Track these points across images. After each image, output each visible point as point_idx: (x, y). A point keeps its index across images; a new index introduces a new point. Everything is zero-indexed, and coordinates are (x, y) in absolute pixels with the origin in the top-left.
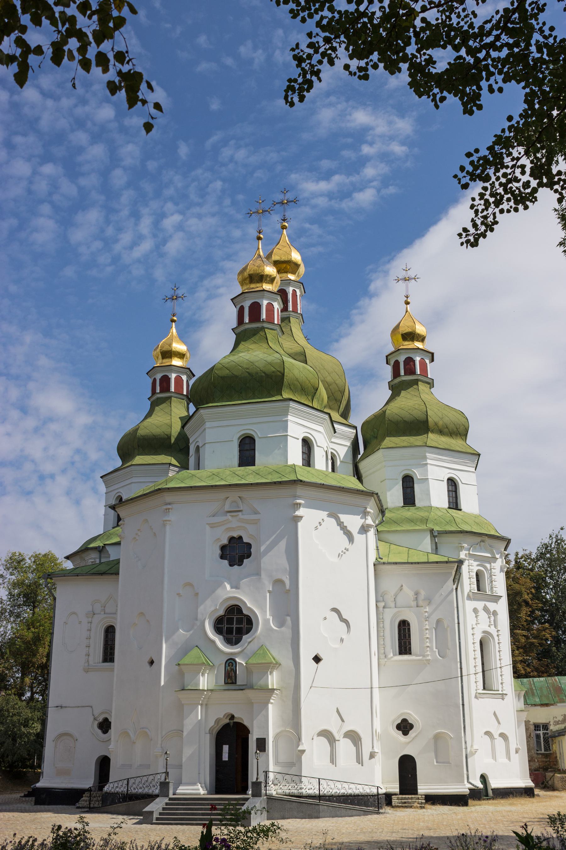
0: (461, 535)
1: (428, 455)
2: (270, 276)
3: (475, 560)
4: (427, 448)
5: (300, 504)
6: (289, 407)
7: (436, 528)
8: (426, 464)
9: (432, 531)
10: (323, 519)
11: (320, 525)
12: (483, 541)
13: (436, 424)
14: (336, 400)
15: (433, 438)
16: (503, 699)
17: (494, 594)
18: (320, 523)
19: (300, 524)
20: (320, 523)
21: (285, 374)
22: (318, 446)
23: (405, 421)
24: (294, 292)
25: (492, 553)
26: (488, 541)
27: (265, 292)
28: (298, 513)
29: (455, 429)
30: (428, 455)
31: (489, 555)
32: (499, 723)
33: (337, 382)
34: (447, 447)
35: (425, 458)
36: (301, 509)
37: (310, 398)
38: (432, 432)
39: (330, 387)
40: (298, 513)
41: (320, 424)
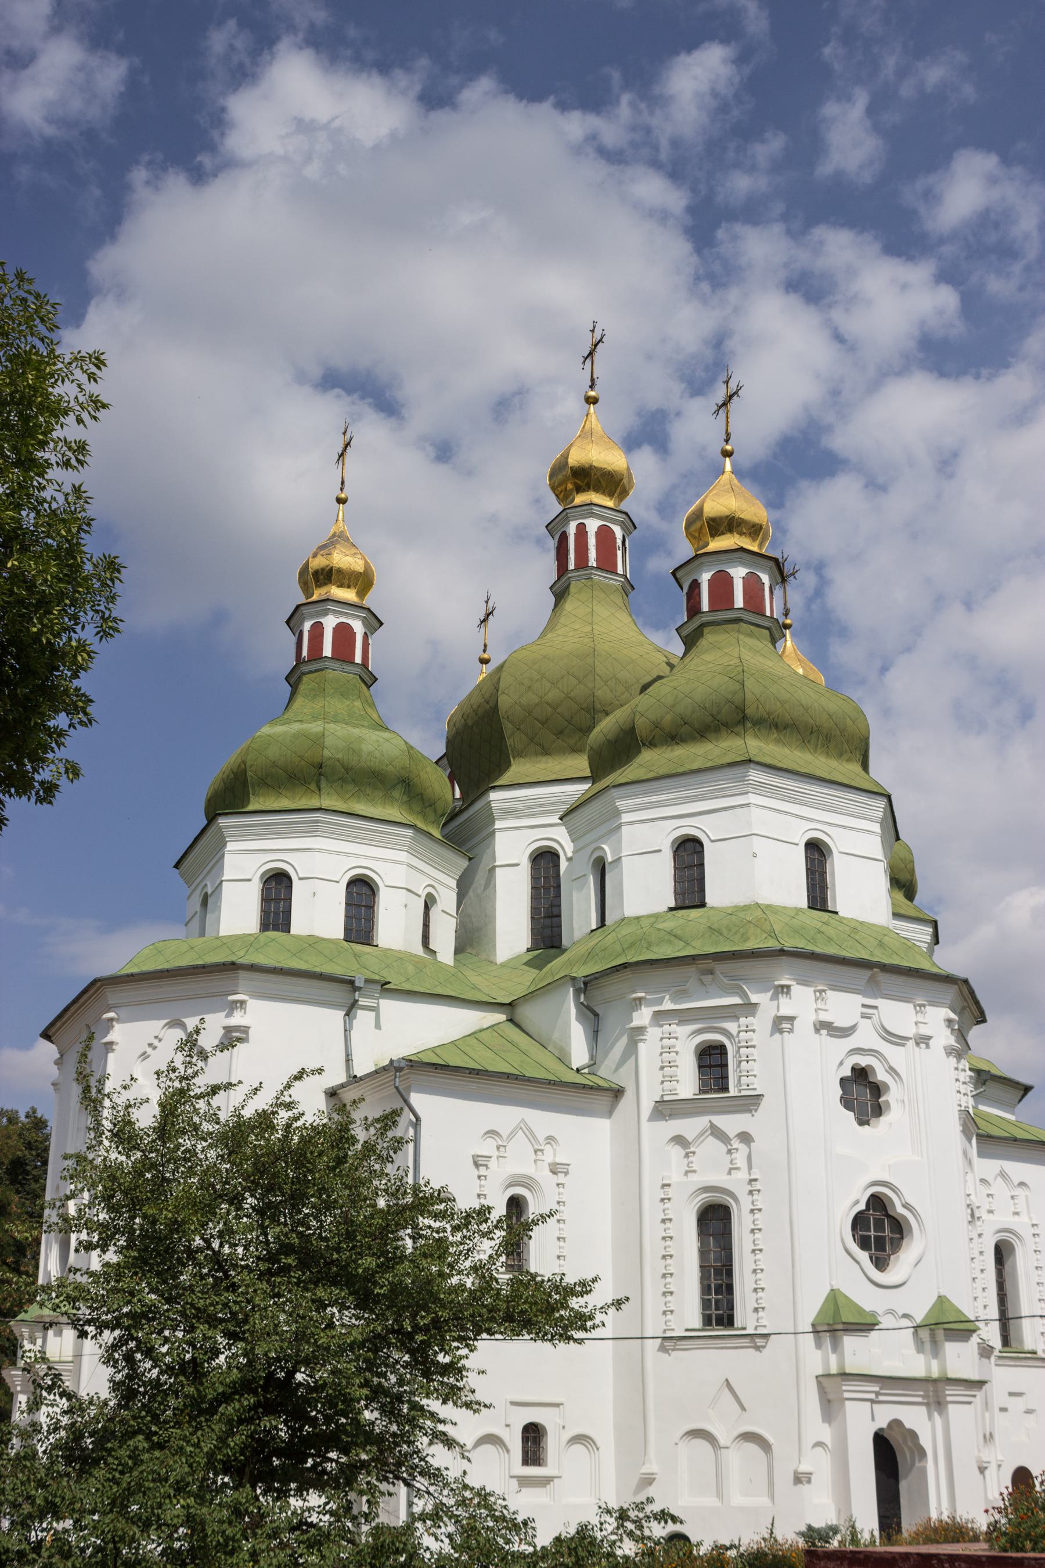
0: (627, 974)
1: (620, 804)
2: (323, 569)
3: (681, 1022)
4: (613, 790)
5: (112, 1020)
6: (220, 828)
7: (581, 972)
8: (619, 826)
9: (574, 979)
10: (156, 1037)
11: (155, 1048)
12: (711, 972)
13: (656, 725)
14: (581, 730)
15: (649, 760)
16: (758, 1348)
17: (743, 1093)
18: (150, 1045)
19: (111, 1056)
20: (150, 1045)
21: (248, 764)
22: (300, 879)
23: (608, 741)
24: (582, 529)
25: (744, 995)
26: (720, 968)
27: (302, 608)
28: (108, 1039)
29: (710, 718)
30: (620, 804)
31: (736, 1000)
32: (743, 1409)
33: (572, 695)
34: (662, 771)
35: (617, 813)
36: (117, 1026)
37: (313, 787)
38: (652, 744)
39: (559, 710)
40: (108, 1039)
41: (313, 831)
